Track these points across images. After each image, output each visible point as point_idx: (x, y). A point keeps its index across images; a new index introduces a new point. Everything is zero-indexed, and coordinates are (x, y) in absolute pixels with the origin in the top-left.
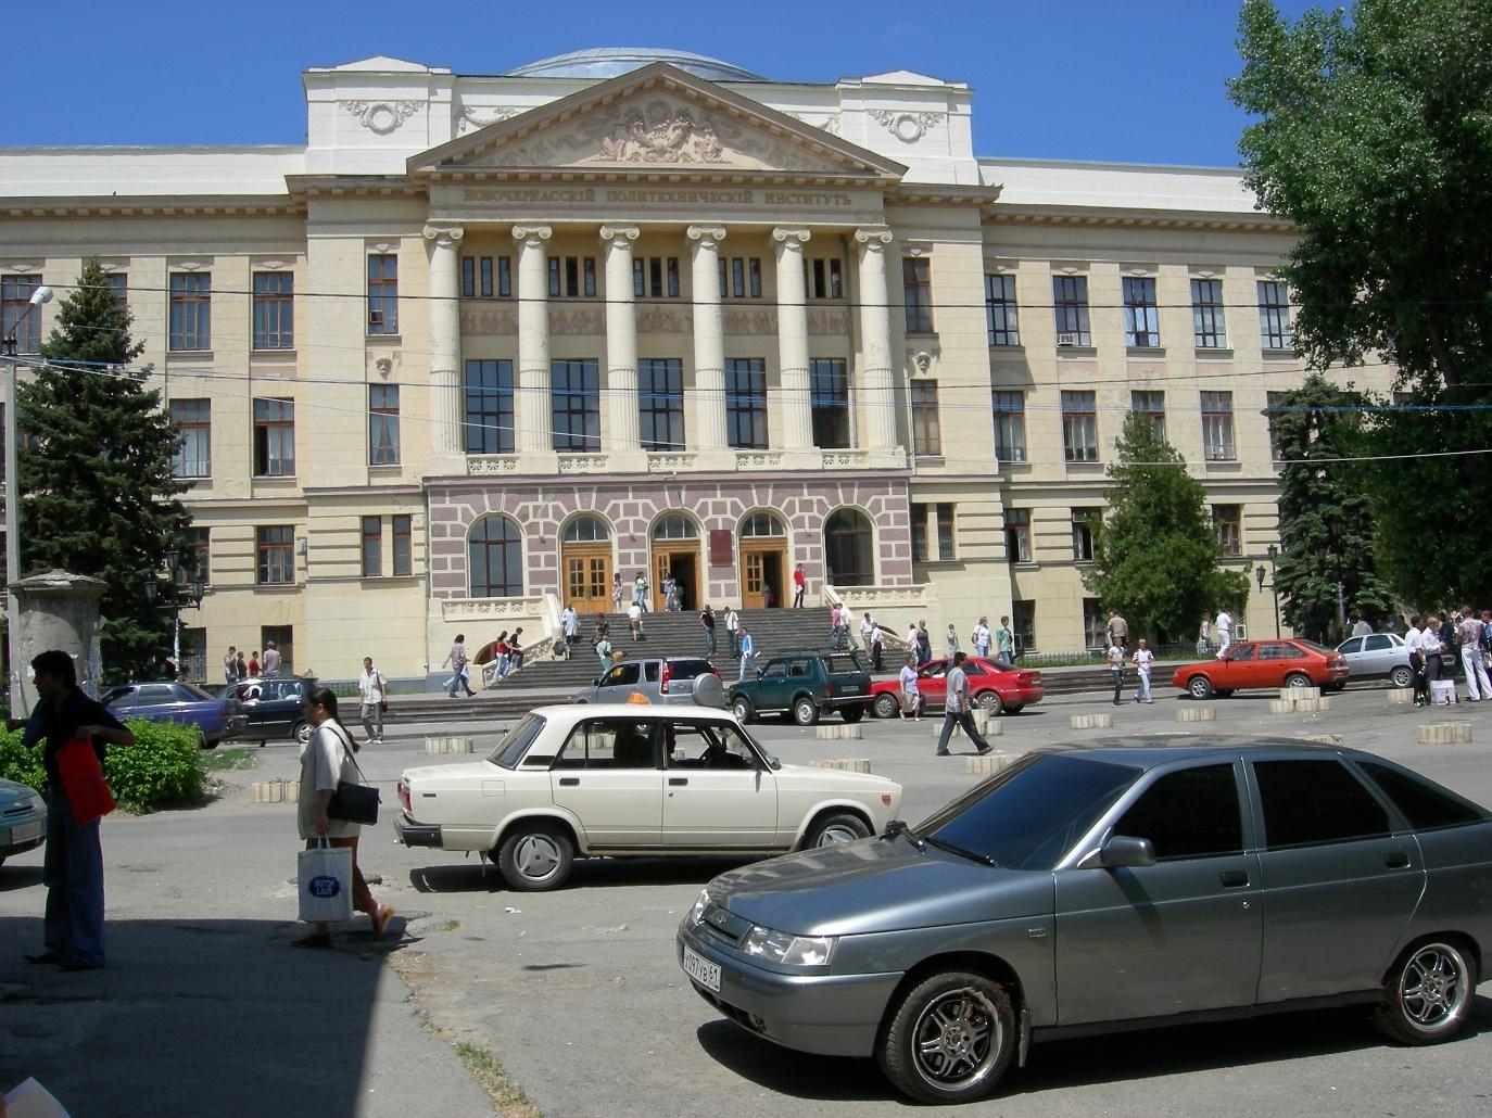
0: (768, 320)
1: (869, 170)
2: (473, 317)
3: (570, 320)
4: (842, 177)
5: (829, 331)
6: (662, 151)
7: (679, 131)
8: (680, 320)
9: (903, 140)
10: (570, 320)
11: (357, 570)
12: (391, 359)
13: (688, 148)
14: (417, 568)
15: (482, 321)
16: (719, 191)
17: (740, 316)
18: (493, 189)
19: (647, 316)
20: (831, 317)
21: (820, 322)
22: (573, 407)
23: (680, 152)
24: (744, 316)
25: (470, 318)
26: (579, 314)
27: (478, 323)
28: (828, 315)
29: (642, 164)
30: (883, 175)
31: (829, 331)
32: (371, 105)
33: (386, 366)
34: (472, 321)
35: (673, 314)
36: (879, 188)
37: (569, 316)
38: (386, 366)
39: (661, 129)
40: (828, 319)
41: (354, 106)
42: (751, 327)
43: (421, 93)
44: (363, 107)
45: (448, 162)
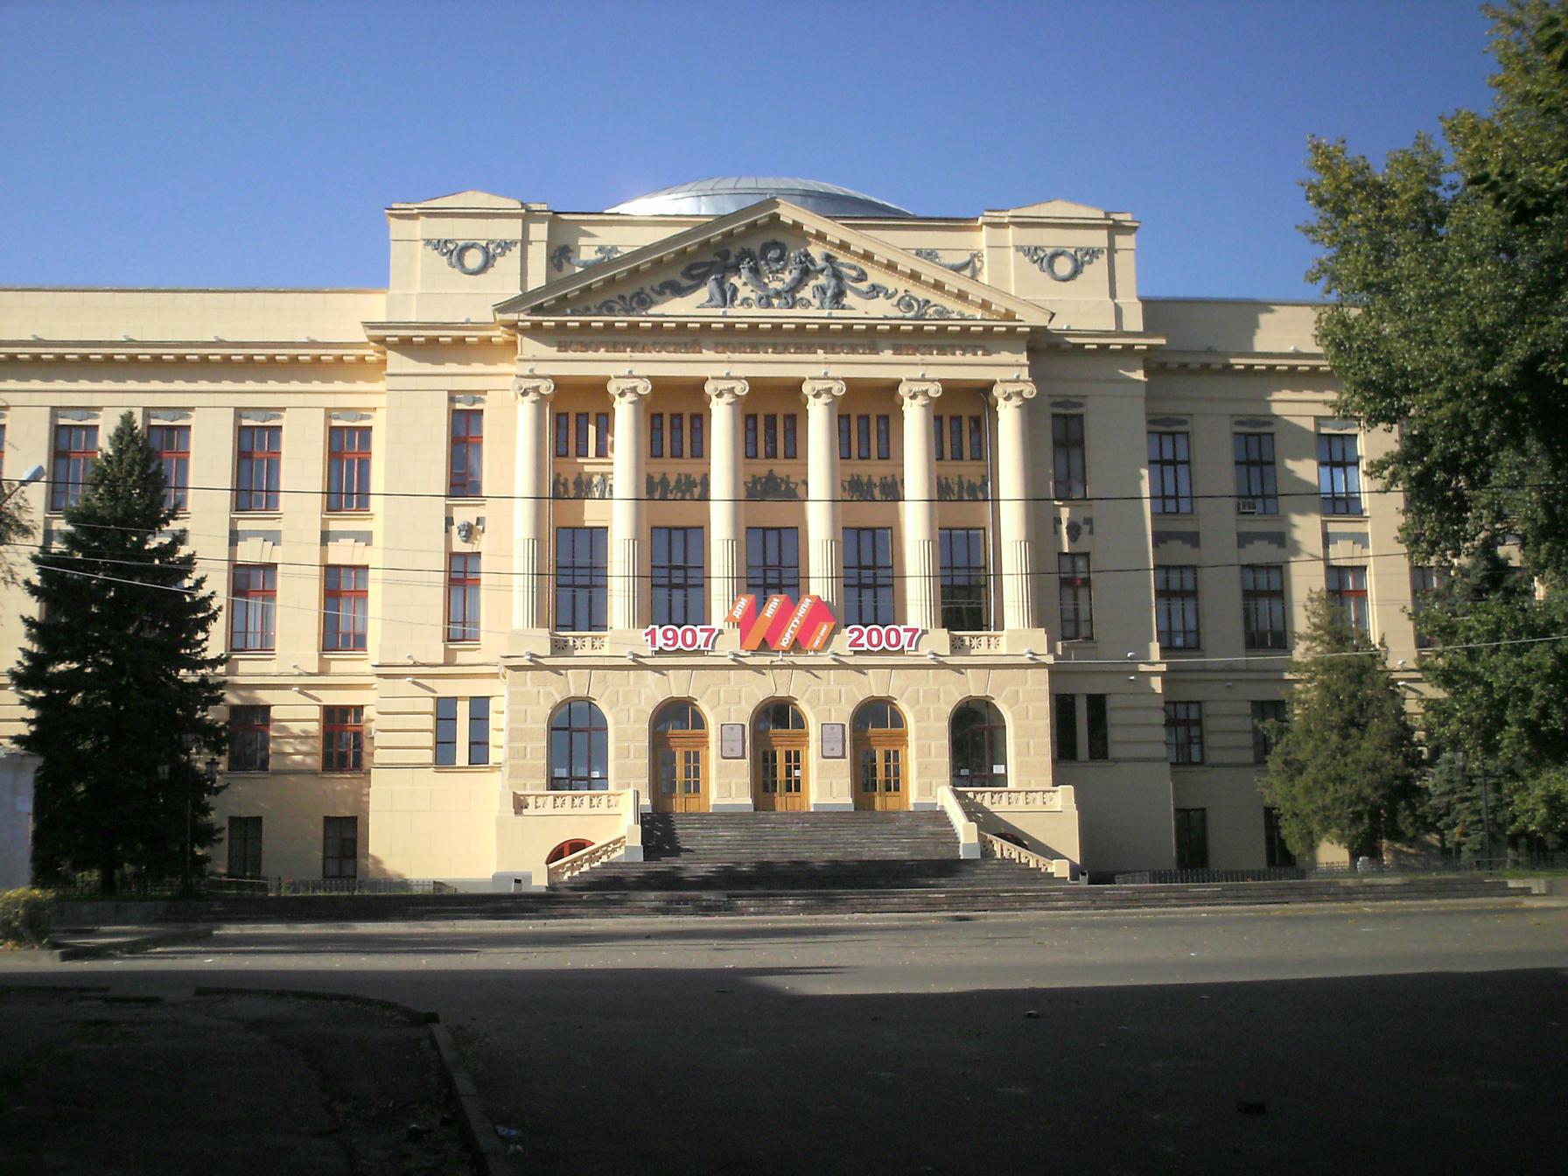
0: (896, 484)
2: (566, 480)
3: (673, 484)
5: (966, 497)
8: (797, 485)
9: (1065, 280)
10: (673, 484)
14: (495, 755)
15: (575, 483)
16: (839, 341)
17: (865, 480)
18: (586, 339)
19: (760, 478)
21: (956, 488)
22: (675, 581)
26: (683, 477)
27: (571, 486)
28: (965, 480)
29: (755, 311)
31: (966, 497)
33: (469, 532)
34: (565, 485)
35: (788, 477)
36: (1023, 334)
37: (672, 481)
38: (469, 532)
39: (777, 271)
40: (965, 485)
41: (439, 245)
42: (877, 493)
43: (512, 229)
44: (451, 247)
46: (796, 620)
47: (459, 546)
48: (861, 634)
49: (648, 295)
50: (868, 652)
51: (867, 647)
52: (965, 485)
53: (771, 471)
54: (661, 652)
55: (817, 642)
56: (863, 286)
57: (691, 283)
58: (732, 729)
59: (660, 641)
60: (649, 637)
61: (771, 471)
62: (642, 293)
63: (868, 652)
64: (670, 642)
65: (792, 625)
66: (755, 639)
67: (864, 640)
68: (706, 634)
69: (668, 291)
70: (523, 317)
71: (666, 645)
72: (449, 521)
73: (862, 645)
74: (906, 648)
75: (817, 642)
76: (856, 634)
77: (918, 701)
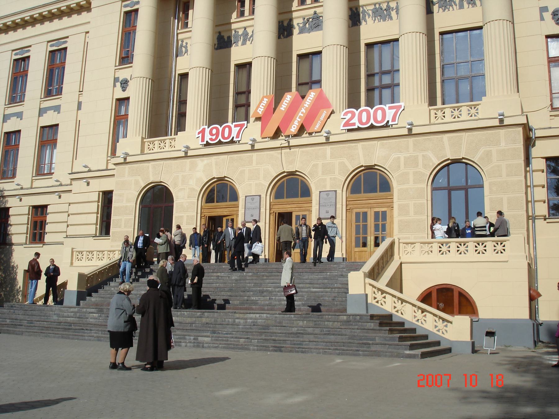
2: (187, 43)
11: (92, 230)
12: (129, 79)
17: (384, 6)
25: (184, 44)
46: (303, 110)
48: (353, 115)
50: (359, 129)
51: (358, 125)
54: (208, 144)
55: (317, 126)
58: (253, 199)
59: (208, 137)
60: (200, 135)
63: (359, 129)
64: (214, 137)
65: (300, 114)
66: (271, 130)
67: (355, 120)
68: (238, 128)
71: (211, 139)
72: (116, 80)
73: (354, 124)
74: (390, 123)
75: (317, 126)
76: (349, 115)
77: (399, 167)
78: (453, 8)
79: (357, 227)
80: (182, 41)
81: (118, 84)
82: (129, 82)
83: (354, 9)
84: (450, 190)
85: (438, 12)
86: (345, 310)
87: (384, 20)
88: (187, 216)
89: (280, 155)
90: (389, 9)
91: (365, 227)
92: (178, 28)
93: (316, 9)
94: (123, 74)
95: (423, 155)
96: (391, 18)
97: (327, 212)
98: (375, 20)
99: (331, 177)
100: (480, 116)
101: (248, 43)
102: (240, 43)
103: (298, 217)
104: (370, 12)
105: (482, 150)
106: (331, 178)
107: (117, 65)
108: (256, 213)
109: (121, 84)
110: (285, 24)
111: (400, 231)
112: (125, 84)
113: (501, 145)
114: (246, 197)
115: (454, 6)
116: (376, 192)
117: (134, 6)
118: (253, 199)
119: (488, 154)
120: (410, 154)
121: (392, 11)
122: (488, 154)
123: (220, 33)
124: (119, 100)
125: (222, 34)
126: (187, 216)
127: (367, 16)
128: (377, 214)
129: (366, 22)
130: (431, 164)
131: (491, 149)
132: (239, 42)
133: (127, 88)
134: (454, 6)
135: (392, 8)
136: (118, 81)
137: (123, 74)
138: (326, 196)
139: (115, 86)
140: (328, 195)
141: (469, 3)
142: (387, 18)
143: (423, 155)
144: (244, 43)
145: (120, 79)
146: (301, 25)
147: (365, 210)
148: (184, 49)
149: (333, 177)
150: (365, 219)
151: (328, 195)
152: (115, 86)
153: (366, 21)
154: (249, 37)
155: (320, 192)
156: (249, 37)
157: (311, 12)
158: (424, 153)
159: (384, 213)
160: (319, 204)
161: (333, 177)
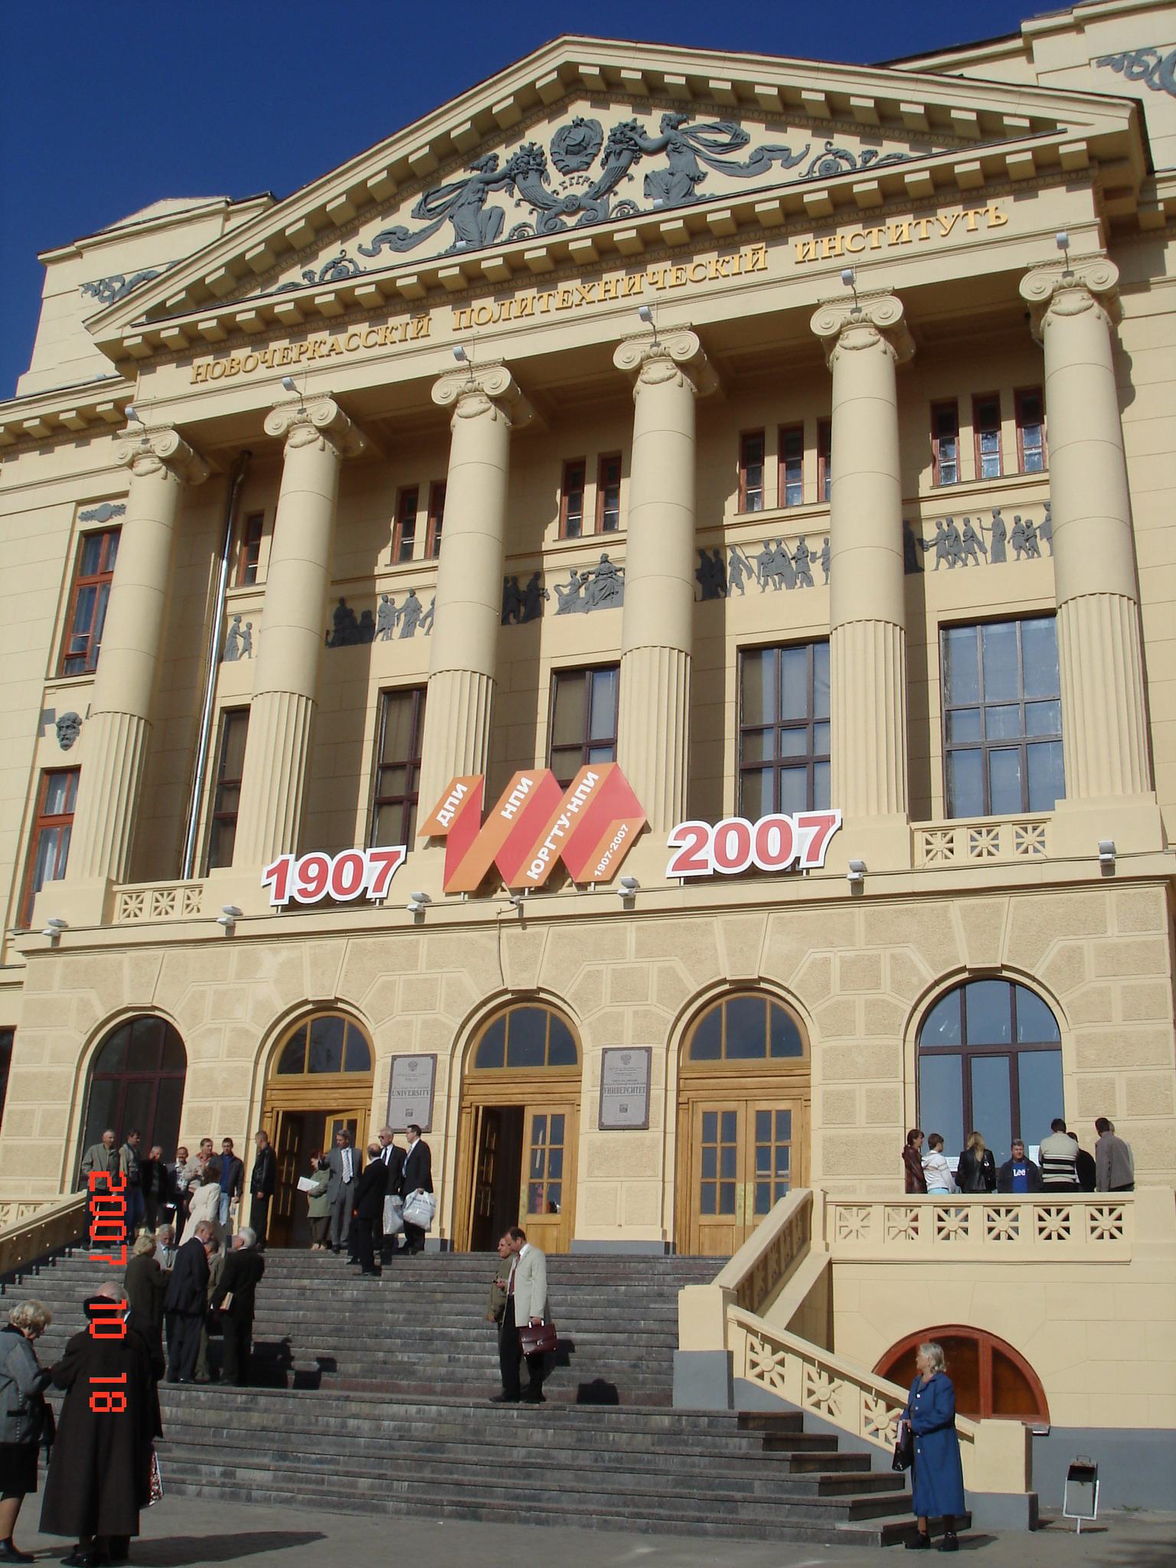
1: (1040, 126)
2: (250, 626)
4: (966, 162)
6: (573, 206)
7: (613, 162)
12: (82, 716)
13: (630, 190)
17: (792, 548)
20: (1018, 520)
21: (988, 539)
23: (613, 201)
24: (802, 549)
25: (243, 628)
28: (1008, 520)
30: (1074, 132)
32: (128, 278)
40: (1010, 527)
45: (158, 313)
46: (564, 821)
47: (55, 757)
48: (702, 839)
49: (351, 261)
50: (717, 878)
51: (713, 865)
52: (1010, 527)
53: (605, 559)
54: (293, 906)
55: (602, 867)
56: (741, 156)
57: (426, 223)
58: (413, 1067)
59: (294, 886)
60: (274, 879)
61: (605, 559)
62: (343, 259)
63: (717, 878)
64: (311, 887)
65: (555, 831)
66: (473, 872)
67: (707, 853)
69: (385, 247)
70: (129, 331)
71: (304, 892)
72: (46, 716)
73: (703, 864)
74: (803, 864)
75: (602, 867)
76: (691, 840)
77: (826, 987)
78: (976, 559)
79: (708, 1155)
80: (238, 620)
81: (51, 729)
82: (80, 724)
83: (710, 554)
84: (968, 1054)
85: (937, 569)
86: (668, 1399)
87: (791, 585)
88: (224, 1109)
89: (496, 943)
90: (803, 555)
91: (730, 1155)
92: (227, 585)
93: (607, 550)
94: (68, 701)
95: (893, 956)
96: (810, 582)
97: (624, 1109)
98: (766, 583)
99: (636, 1008)
100: (1049, 852)
101: (419, 631)
102: (397, 631)
103: (539, 1121)
104: (754, 563)
105: (1056, 946)
106: (636, 1013)
107: (52, 674)
108: (421, 1104)
109: (60, 728)
110: (523, 585)
111: (829, 1169)
112: (69, 728)
113: (1109, 934)
114: (394, 1058)
115: (980, 555)
116: (762, 1055)
117: (111, 517)
118: (413, 1067)
119: (1073, 956)
120: (857, 953)
121: (813, 562)
122: (1073, 956)
123: (342, 601)
124: (48, 772)
125: (349, 606)
126: (224, 1109)
127: (744, 574)
128: (763, 1117)
129: (742, 588)
130: (915, 981)
131: (1080, 943)
132: (395, 628)
133: (74, 739)
134: (980, 555)
135: (814, 554)
136: (52, 721)
137: (68, 701)
138: (621, 1065)
139: (41, 732)
140: (626, 1060)
141: (1019, 548)
142: (798, 581)
143: (893, 956)
144: (407, 633)
145: (58, 716)
146: (566, 591)
147: (730, 1106)
148: (240, 641)
149: (642, 1008)
150: (730, 1133)
151: (626, 1060)
152: (41, 732)
153: (740, 586)
154: (422, 616)
155: (605, 1051)
156: (422, 616)
157: (595, 555)
158: (898, 951)
159: (784, 1117)
160: (602, 1081)
161: (642, 1008)
